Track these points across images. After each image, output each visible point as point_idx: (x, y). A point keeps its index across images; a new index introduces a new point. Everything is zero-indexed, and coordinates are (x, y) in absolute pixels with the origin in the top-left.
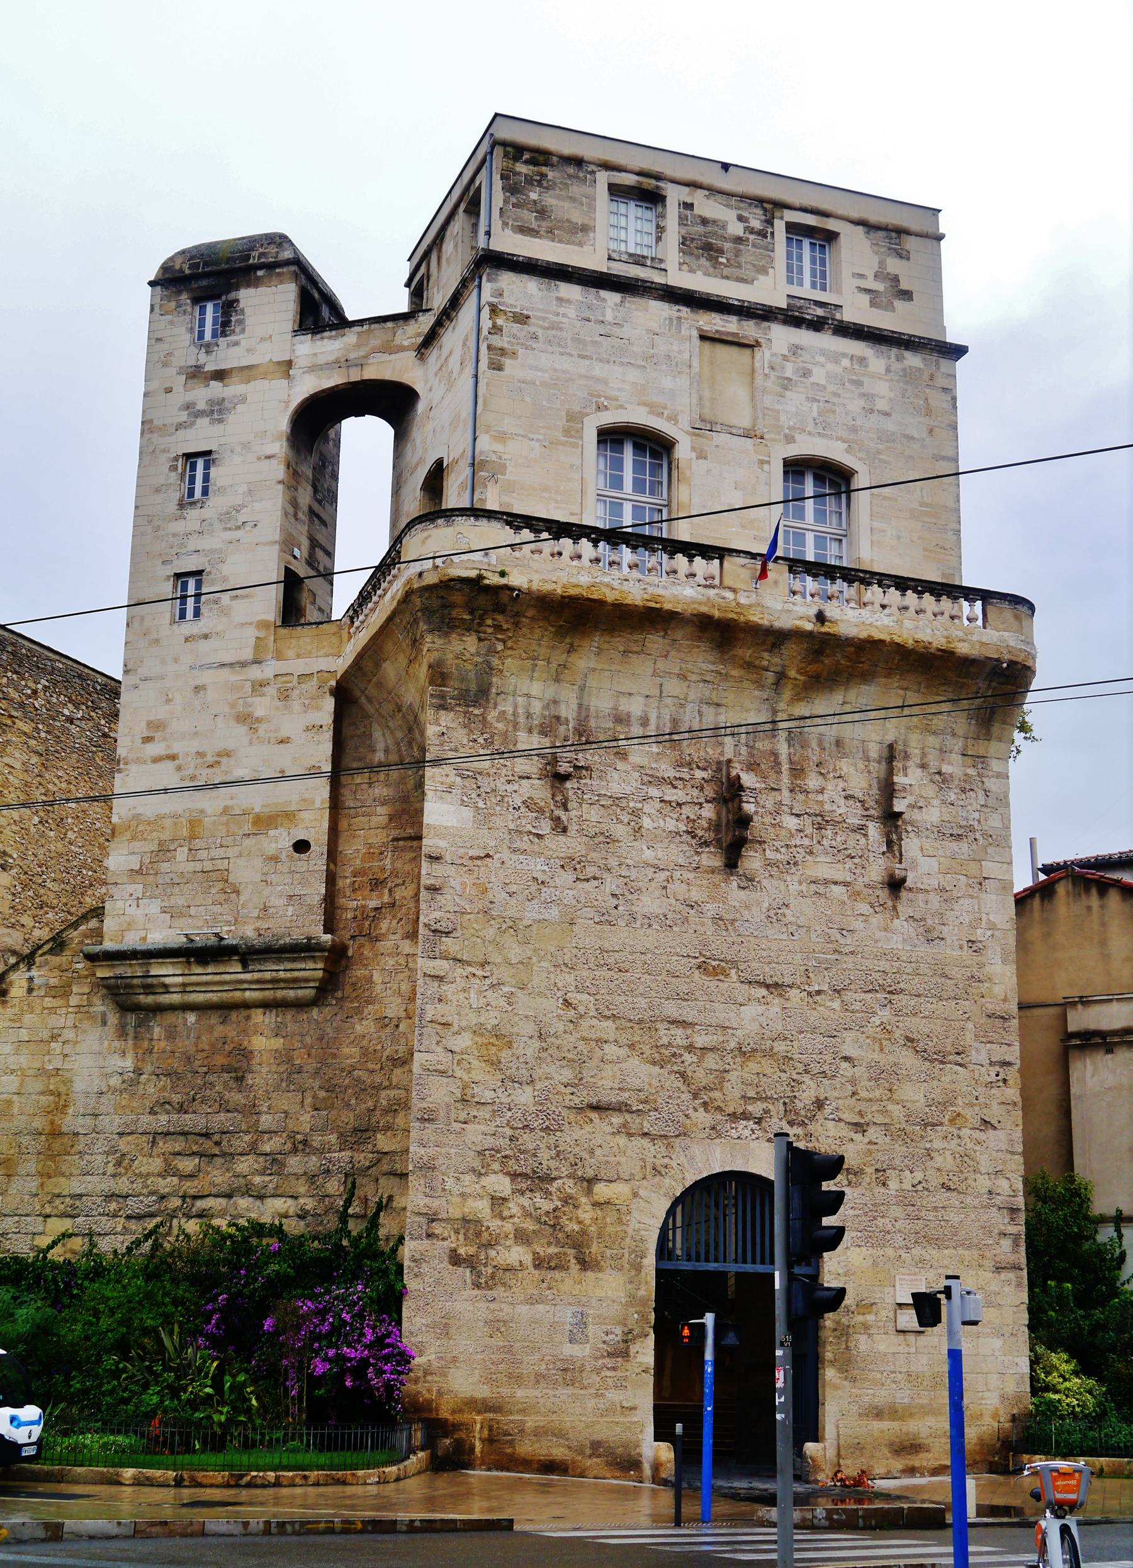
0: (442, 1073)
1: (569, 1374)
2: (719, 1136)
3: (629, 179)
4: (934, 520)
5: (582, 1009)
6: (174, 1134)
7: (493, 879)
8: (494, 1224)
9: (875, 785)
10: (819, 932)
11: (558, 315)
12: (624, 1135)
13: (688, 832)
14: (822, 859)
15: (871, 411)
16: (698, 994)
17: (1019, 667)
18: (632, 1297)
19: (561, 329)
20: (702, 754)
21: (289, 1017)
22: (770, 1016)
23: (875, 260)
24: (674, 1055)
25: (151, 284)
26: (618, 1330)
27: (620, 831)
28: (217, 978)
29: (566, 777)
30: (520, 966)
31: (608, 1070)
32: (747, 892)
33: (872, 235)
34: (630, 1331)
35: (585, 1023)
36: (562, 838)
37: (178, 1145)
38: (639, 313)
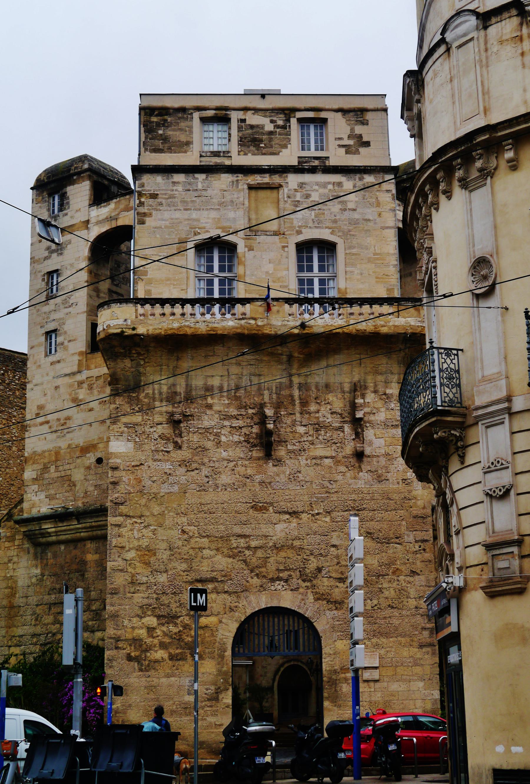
0: (121, 570)
1: (188, 710)
2: (265, 590)
3: (211, 113)
4: (382, 262)
5: (191, 534)
6: (57, 603)
7: (144, 475)
8: (149, 641)
9: (348, 405)
10: (317, 484)
11: (173, 190)
12: (215, 593)
13: (245, 441)
14: (319, 446)
15: (345, 210)
16: (251, 521)
17: (419, 335)
18: (219, 671)
19: (175, 198)
20: (252, 401)
21: (101, 544)
22: (291, 528)
23: (349, 128)
24: (240, 552)
25: (32, 188)
26: (213, 688)
27: (209, 444)
28: (68, 528)
29: (179, 422)
30: (159, 516)
31: (205, 562)
32: (278, 467)
33: (347, 115)
34: (219, 688)
35: (193, 541)
36: (179, 452)
38: (216, 182)
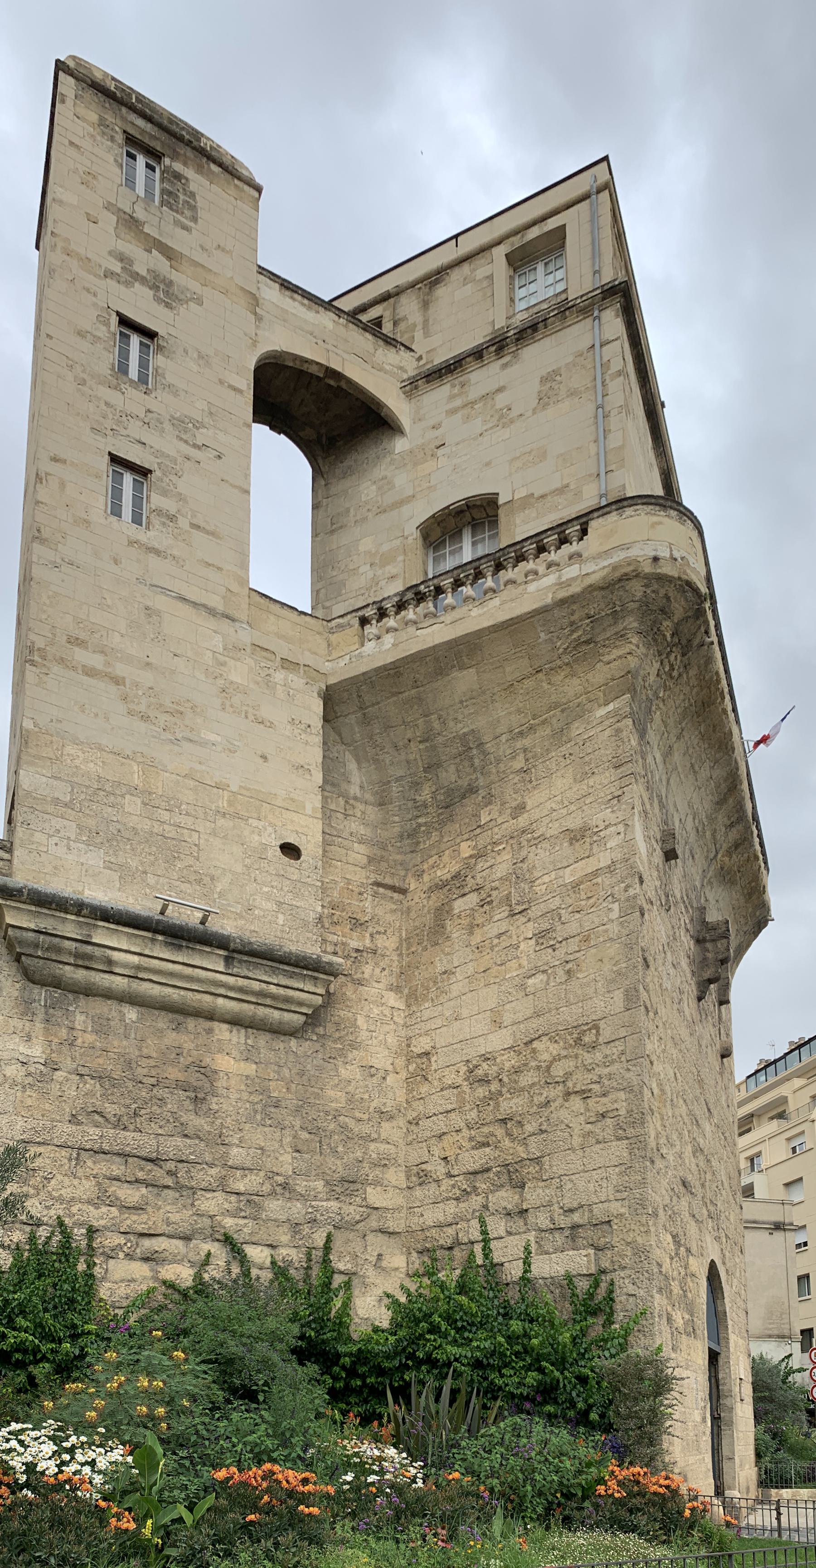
37: (117, 1168)
